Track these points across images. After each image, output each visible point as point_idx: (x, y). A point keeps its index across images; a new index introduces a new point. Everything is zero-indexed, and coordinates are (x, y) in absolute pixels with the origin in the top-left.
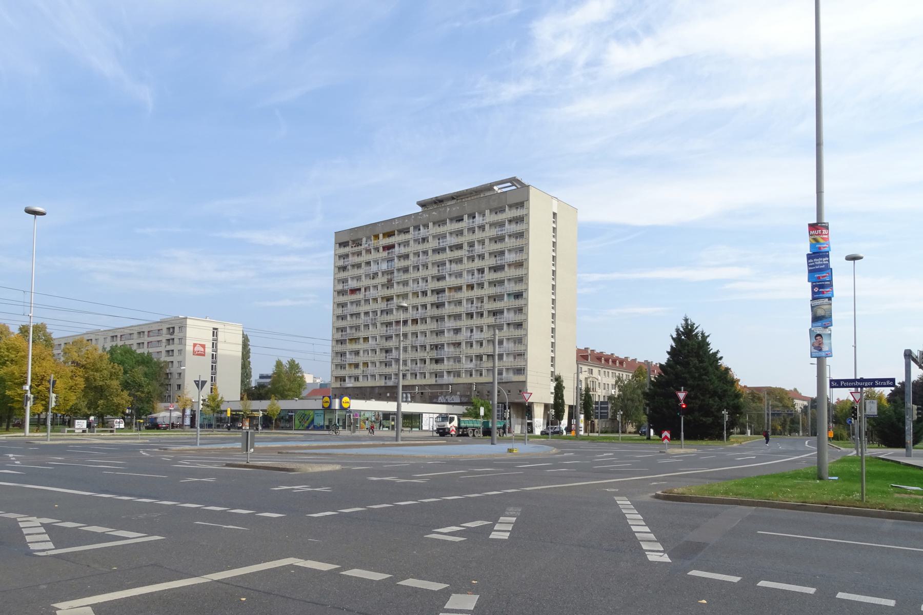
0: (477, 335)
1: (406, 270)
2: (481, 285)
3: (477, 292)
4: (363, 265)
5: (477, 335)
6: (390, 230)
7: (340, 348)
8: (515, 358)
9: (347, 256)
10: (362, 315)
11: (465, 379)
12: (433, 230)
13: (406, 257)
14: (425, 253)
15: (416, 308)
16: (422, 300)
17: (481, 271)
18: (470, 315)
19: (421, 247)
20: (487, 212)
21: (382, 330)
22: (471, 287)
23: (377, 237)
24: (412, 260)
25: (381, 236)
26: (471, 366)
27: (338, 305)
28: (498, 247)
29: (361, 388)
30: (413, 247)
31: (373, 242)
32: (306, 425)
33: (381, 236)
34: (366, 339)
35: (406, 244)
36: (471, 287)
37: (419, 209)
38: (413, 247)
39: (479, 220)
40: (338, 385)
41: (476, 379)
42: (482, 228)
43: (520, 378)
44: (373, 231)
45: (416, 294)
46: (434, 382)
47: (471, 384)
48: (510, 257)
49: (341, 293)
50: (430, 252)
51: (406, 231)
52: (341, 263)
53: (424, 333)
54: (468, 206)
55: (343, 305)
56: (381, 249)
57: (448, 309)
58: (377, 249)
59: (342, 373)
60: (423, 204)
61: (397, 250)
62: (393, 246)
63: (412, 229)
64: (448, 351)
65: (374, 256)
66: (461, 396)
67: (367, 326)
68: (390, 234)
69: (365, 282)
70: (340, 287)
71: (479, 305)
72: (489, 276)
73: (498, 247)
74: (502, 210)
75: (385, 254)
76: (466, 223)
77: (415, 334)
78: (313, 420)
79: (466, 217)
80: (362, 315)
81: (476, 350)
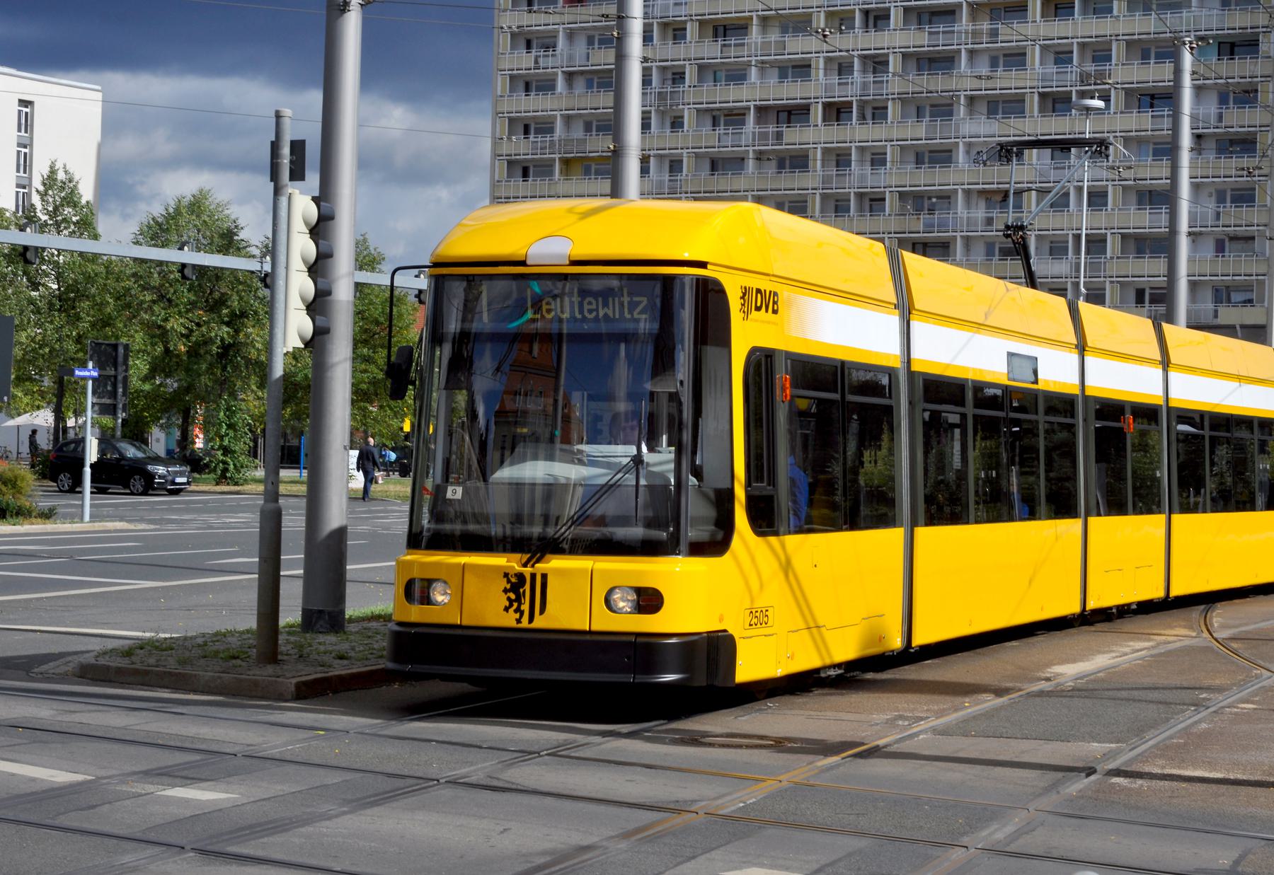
71: (1090, 68)
77: (840, 159)
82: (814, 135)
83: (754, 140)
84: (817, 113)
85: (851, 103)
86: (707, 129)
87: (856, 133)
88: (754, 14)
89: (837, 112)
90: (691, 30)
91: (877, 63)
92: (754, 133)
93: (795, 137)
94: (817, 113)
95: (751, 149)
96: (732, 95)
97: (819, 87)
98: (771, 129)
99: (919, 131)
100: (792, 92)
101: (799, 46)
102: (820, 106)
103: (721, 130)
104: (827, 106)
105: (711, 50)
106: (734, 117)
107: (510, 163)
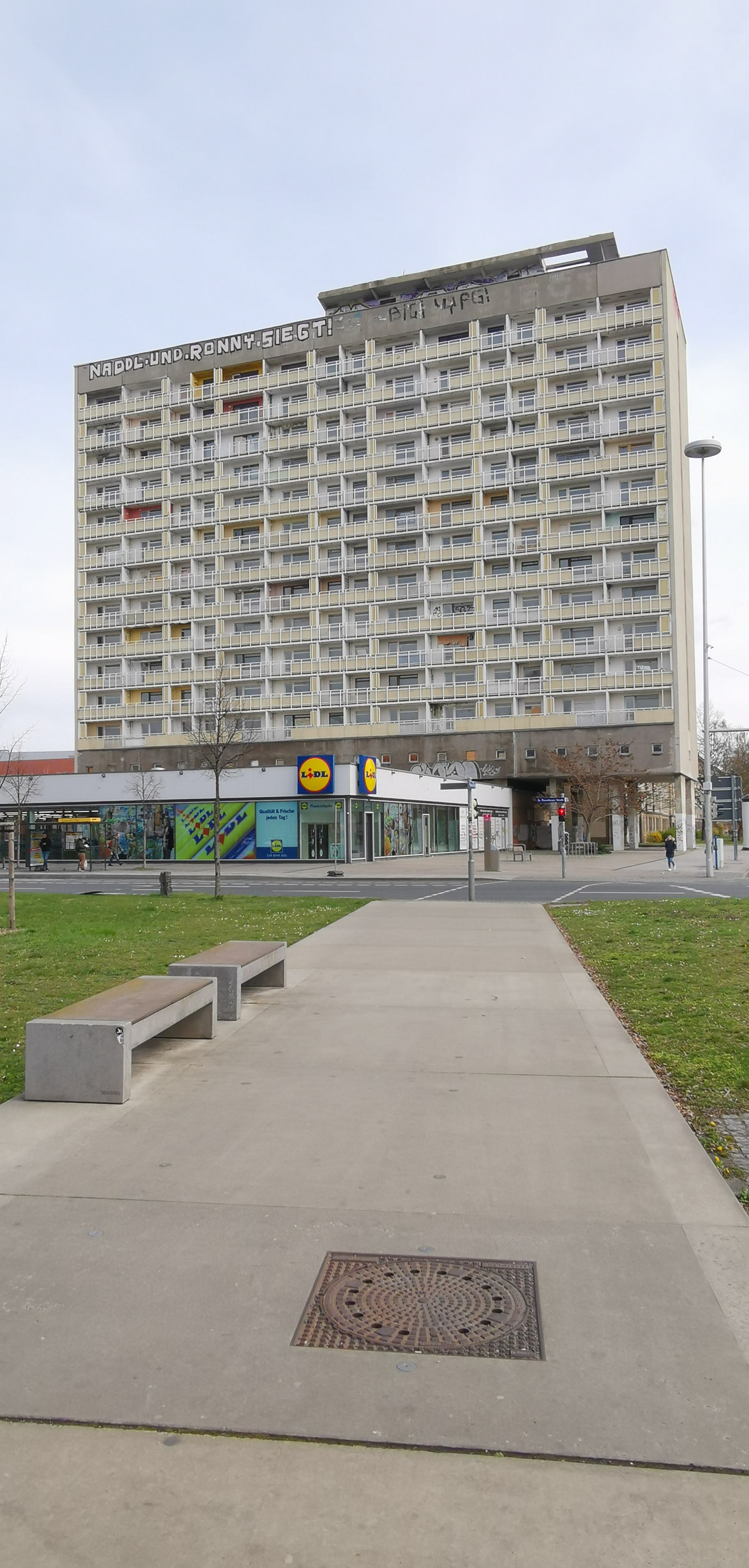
0: (517, 614)
1: (298, 457)
2: (528, 492)
3: (513, 510)
4: (166, 445)
5: (517, 614)
6: (243, 360)
7: (98, 652)
8: (629, 667)
9: (112, 424)
10: (167, 569)
11: (485, 721)
12: (374, 357)
13: (299, 424)
14: (356, 415)
15: (332, 550)
16: (346, 530)
17: (527, 457)
18: (497, 565)
19: (343, 401)
20: (540, 315)
21: (227, 605)
22: (496, 497)
23: (205, 378)
24: (316, 434)
25: (218, 374)
26: (511, 687)
27: (90, 545)
28: (571, 398)
29: (170, 749)
30: (316, 403)
31: (195, 392)
32: (221, 848)
33: (218, 374)
34: (181, 629)
35: (299, 392)
36: (496, 497)
37: (321, 312)
38: (316, 403)
39: (511, 335)
40: (100, 743)
41: (518, 720)
42: (525, 354)
43: (659, 715)
44: (194, 365)
45: (330, 517)
46: (280, 737)
47: (510, 732)
48: (607, 425)
49: (97, 515)
50: (370, 413)
51: (297, 362)
52: (98, 441)
53: (361, 614)
54: (501, 292)
55: (99, 546)
56: (219, 407)
57: (429, 551)
58: (207, 410)
59: (108, 713)
60: (331, 302)
61: (273, 410)
62: (255, 401)
63: (311, 357)
64: (432, 654)
65: (196, 423)
66: (480, 764)
67: (183, 598)
68: (250, 370)
69: (170, 488)
70: (98, 501)
72: (547, 468)
73: (571, 398)
74: (576, 310)
75: (233, 418)
76: (477, 340)
77: (332, 615)
78: (252, 833)
79: (475, 328)
80: (167, 569)
81: (518, 649)
82: (313, 600)
83: (268, 607)
84: (315, 585)
85: (340, 576)
86: (232, 601)
87: (346, 596)
88: (265, 517)
89: (329, 582)
90: (219, 531)
91: (358, 546)
92: (267, 602)
93: (298, 602)
94: (315, 585)
95: (265, 614)
96: (249, 576)
97: (317, 565)
98: (281, 598)
99: (393, 593)
100: (294, 571)
101: (297, 538)
102: (317, 580)
103: (242, 601)
104: (322, 580)
105: (234, 544)
106: (252, 591)
107: (89, 634)
